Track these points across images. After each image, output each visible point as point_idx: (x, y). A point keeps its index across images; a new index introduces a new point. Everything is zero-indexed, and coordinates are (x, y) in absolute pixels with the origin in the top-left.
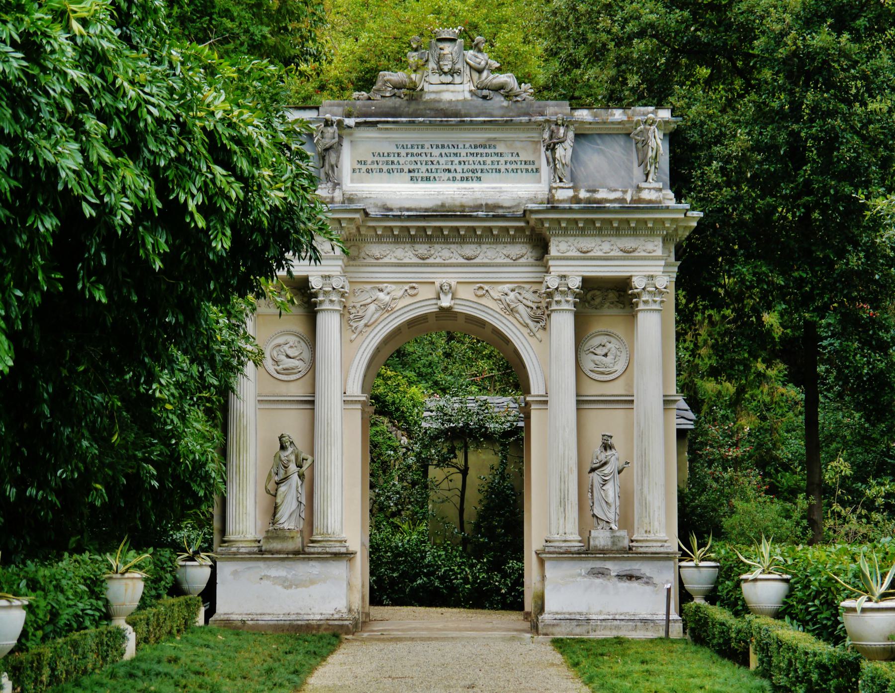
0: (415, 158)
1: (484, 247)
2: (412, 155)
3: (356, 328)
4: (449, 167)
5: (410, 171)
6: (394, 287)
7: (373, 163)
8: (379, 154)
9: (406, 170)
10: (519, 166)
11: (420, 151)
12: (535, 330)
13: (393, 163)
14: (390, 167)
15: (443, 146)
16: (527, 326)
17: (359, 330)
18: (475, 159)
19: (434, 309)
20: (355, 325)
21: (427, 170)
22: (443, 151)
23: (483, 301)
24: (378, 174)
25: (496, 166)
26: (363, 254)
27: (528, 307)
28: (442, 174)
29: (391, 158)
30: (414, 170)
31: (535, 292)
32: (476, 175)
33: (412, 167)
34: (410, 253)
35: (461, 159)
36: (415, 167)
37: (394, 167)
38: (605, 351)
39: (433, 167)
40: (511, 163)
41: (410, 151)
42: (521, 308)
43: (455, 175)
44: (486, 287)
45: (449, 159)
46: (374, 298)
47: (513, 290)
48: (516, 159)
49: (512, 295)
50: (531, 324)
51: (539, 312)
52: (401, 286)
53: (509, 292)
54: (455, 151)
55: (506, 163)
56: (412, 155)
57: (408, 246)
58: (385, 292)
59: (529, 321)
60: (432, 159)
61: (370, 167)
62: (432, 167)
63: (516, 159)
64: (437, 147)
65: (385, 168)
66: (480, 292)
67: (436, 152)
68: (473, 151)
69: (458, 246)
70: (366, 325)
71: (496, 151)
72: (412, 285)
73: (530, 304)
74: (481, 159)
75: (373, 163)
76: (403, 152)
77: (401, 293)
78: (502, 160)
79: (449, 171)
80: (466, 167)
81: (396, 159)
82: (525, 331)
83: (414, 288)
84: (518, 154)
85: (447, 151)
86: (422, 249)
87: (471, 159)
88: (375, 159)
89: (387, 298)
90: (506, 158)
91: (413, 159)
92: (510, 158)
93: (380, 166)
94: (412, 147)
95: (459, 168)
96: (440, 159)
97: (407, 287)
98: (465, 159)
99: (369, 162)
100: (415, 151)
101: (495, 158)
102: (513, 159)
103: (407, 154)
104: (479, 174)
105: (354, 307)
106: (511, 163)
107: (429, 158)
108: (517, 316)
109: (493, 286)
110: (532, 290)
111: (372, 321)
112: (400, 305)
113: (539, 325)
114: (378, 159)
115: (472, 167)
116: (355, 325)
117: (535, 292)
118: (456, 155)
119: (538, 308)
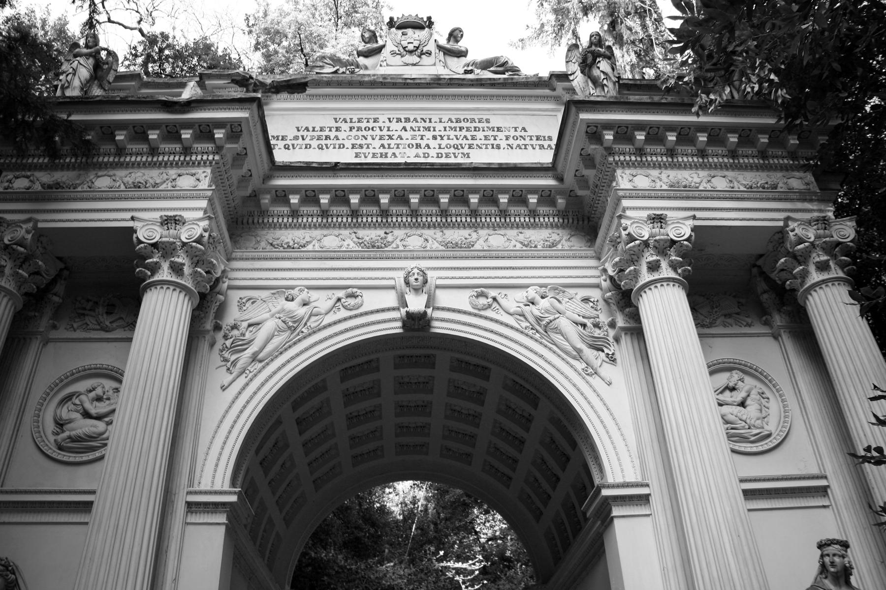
0: (364, 133)
1: (483, 232)
2: (359, 129)
3: (234, 363)
4: (419, 141)
5: (353, 146)
6: (314, 295)
7: (296, 138)
8: (307, 129)
9: (348, 144)
10: (527, 142)
11: (371, 125)
12: (597, 363)
13: (327, 137)
14: (323, 142)
15: (407, 120)
16: (579, 355)
17: (239, 365)
18: (458, 133)
19: (395, 328)
20: (233, 358)
21: (383, 146)
22: (408, 125)
23: (489, 313)
24: (303, 150)
25: (492, 141)
26: (263, 244)
27: (577, 324)
28: (407, 150)
29: (327, 133)
30: (361, 146)
31: (586, 300)
32: (461, 151)
33: (359, 142)
34: (348, 241)
35: (437, 133)
36: (364, 142)
37: (328, 142)
38: (738, 396)
39: (392, 142)
40: (515, 138)
41: (357, 125)
42: (564, 323)
43: (426, 150)
44: (493, 293)
45: (417, 133)
46: (274, 310)
47: (543, 298)
48: (523, 134)
49: (544, 303)
50: (589, 353)
51: (597, 333)
52: (330, 292)
53: (538, 298)
54: (427, 124)
55: (507, 139)
56: (359, 129)
57: (345, 232)
58: (298, 300)
59: (580, 345)
60: (390, 133)
61: (290, 143)
62: (390, 141)
63: (523, 134)
64: (399, 120)
65: (315, 143)
66: (482, 301)
67: (394, 126)
68: (453, 125)
69: (438, 231)
70: (254, 358)
71: (490, 125)
72: (350, 290)
73: (581, 319)
74: (468, 134)
75: (296, 138)
76: (345, 126)
77: (330, 303)
78: (501, 135)
79: (418, 146)
80: (444, 143)
81: (332, 134)
82: (580, 366)
83: (353, 296)
84: (524, 129)
85: (414, 125)
86: (371, 235)
87: (452, 134)
88: (300, 134)
89: (302, 311)
90: (507, 133)
91: (360, 133)
92: (512, 133)
93: (307, 141)
94: (360, 121)
95: (433, 144)
96: (403, 134)
97: (341, 294)
98: (442, 133)
99: (290, 136)
100: (363, 125)
101: (490, 133)
102: (518, 134)
103: (351, 129)
104: (466, 150)
105: (235, 327)
106: (515, 138)
107: (385, 132)
108: (557, 338)
109: (504, 291)
110: (579, 297)
111: (270, 347)
112: (328, 319)
113: (603, 355)
114: (305, 133)
115: (455, 142)
116: (233, 358)
117: (586, 300)
118: (428, 129)
119: (597, 325)
